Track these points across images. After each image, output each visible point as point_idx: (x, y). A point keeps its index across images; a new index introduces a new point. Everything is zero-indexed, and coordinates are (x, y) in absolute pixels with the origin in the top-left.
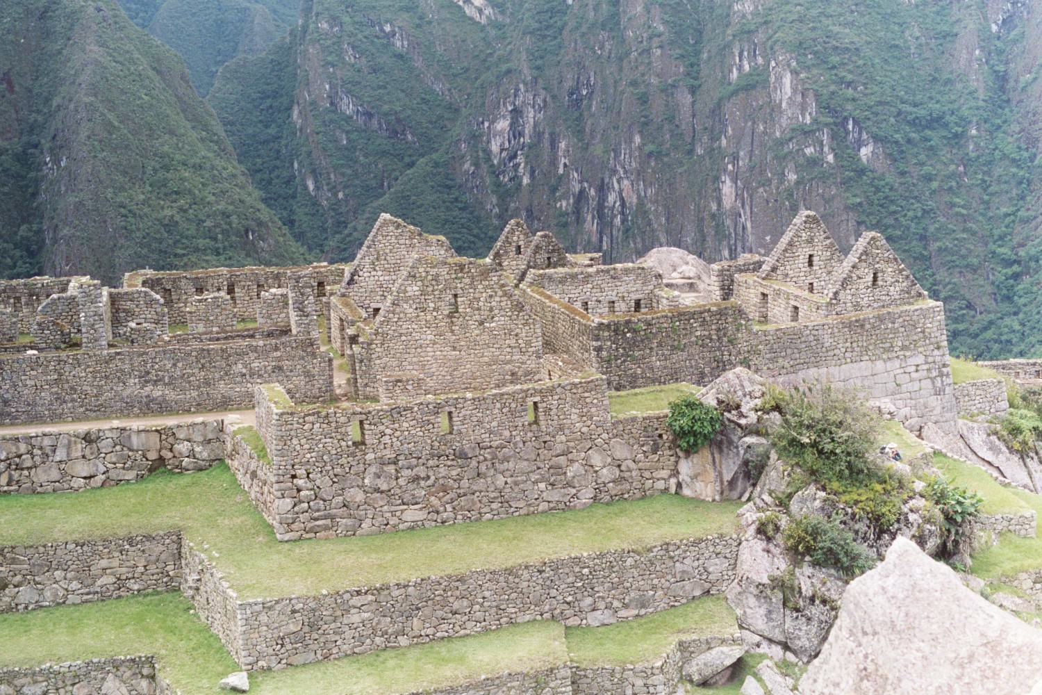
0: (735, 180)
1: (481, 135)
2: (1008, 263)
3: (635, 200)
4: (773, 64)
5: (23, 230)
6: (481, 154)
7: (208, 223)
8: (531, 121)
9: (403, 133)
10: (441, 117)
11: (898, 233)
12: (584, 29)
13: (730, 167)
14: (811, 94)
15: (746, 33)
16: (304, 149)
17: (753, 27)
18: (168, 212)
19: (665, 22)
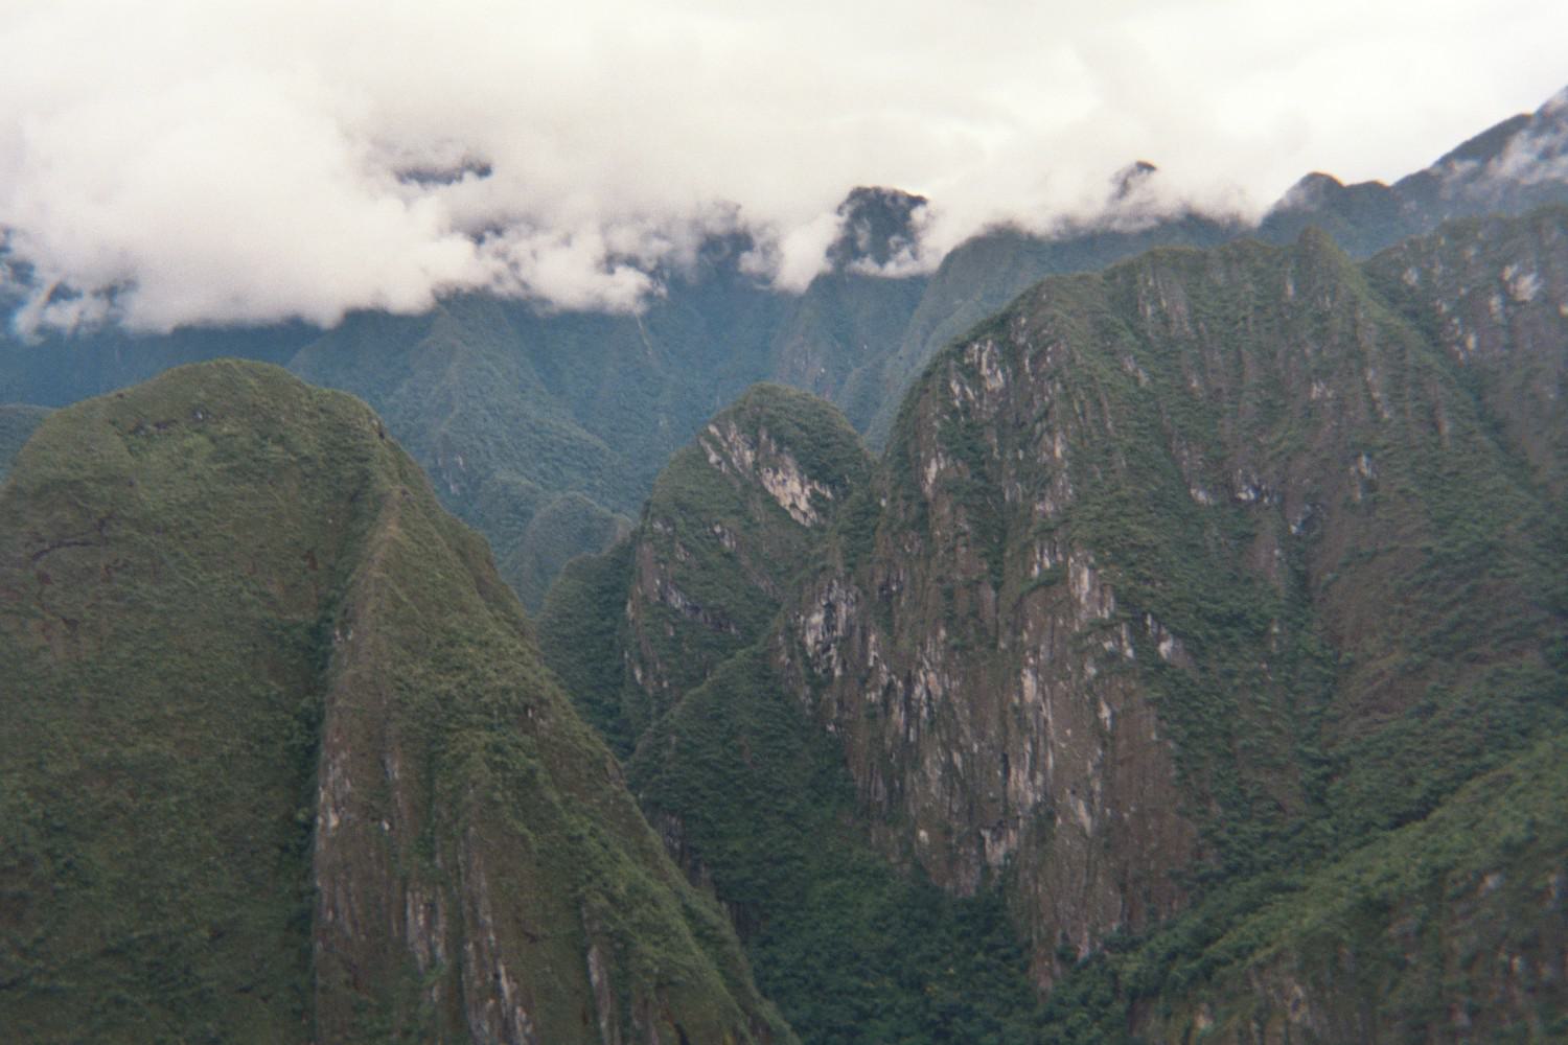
0: (1036, 673)
1: (798, 628)
2: (1317, 763)
3: (940, 693)
4: (1071, 560)
5: (305, 703)
6: (796, 647)
7: (486, 699)
8: (844, 615)
9: (728, 627)
10: (764, 612)
11: (1201, 729)
12: (895, 528)
13: (1031, 661)
14: (1109, 589)
15: (1047, 532)
16: (634, 640)
17: (1052, 526)
18: (444, 687)
19: (969, 521)
